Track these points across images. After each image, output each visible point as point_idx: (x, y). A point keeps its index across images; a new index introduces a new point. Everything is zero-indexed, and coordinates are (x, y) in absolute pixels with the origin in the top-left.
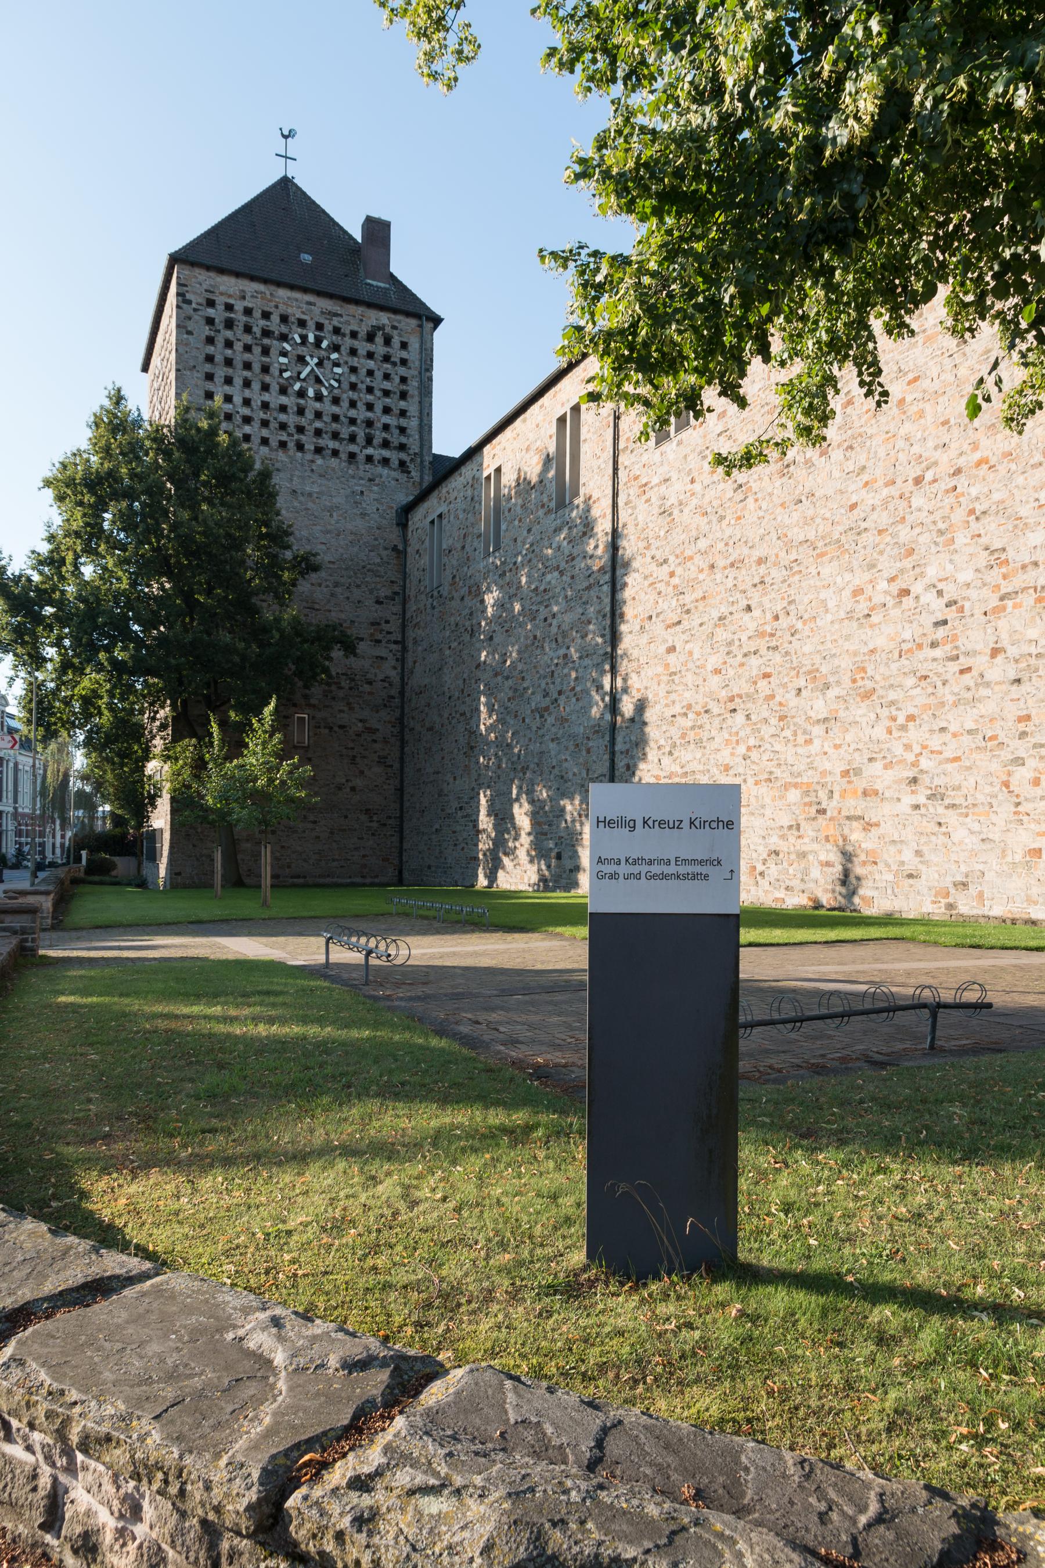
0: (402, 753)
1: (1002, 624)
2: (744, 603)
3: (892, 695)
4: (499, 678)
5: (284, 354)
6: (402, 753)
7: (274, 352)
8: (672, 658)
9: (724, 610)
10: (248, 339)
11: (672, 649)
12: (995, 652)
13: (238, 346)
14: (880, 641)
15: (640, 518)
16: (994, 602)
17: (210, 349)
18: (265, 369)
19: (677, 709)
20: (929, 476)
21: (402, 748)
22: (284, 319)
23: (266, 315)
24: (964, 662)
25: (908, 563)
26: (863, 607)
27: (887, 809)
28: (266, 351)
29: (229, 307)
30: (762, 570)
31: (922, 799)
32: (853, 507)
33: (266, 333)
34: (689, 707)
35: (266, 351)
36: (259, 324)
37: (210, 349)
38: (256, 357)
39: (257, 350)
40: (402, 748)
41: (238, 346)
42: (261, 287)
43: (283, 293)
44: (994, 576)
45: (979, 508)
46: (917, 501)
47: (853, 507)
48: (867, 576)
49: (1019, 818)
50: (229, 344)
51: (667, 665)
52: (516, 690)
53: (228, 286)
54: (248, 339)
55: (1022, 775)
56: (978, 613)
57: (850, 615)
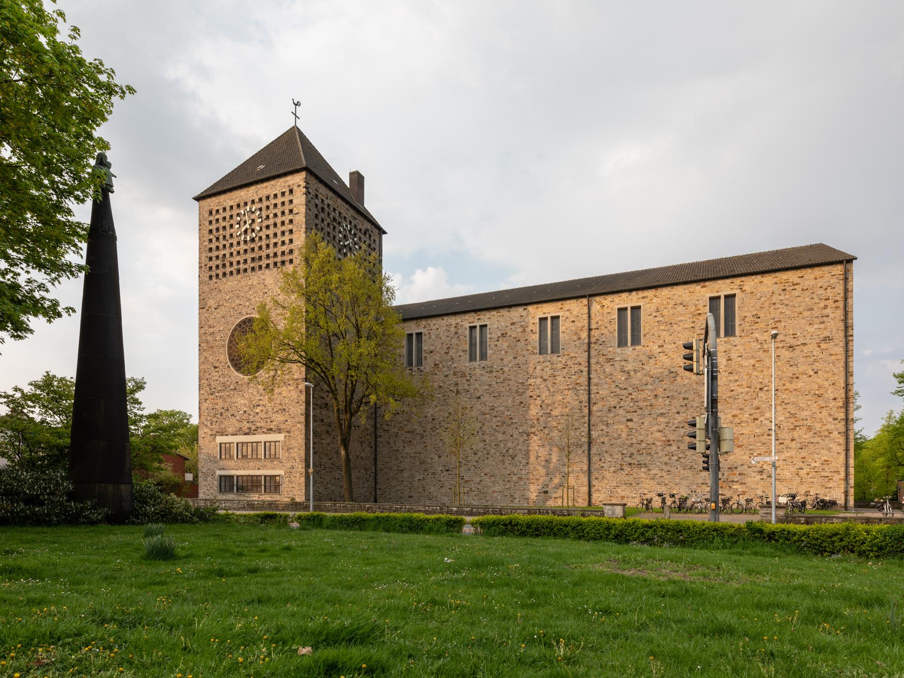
0: (376, 441)
1: (795, 433)
2: (675, 410)
3: (751, 447)
4: (488, 416)
5: (340, 232)
6: (376, 441)
7: (337, 230)
8: (630, 424)
9: (662, 411)
10: (329, 220)
11: (631, 420)
12: (792, 440)
13: (326, 223)
14: (745, 432)
15: (607, 370)
16: (792, 427)
17: (317, 221)
18: (334, 237)
19: (634, 441)
20: (765, 389)
21: (376, 439)
22: (340, 213)
23: (334, 210)
24: (780, 441)
25: (757, 411)
26: (737, 420)
27: (749, 479)
28: (334, 228)
29: (323, 201)
30: (686, 401)
31: (765, 477)
32: (732, 391)
33: (334, 219)
34: (642, 441)
35: (334, 228)
36: (332, 214)
37: (317, 221)
38: (330, 230)
39: (332, 227)
40: (376, 439)
41: (326, 223)
42: (333, 195)
43: (339, 201)
44: (792, 420)
45: (786, 401)
46: (760, 395)
47: (732, 391)
48: (739, 412)
49: (802, 482)
50: (323, 220)
51: (627, 426)
52: (504, 423)
53: (323, 190)
54: (329, 220)
55: (802, 472)
56: (786, 429)
57: (731, 422)
